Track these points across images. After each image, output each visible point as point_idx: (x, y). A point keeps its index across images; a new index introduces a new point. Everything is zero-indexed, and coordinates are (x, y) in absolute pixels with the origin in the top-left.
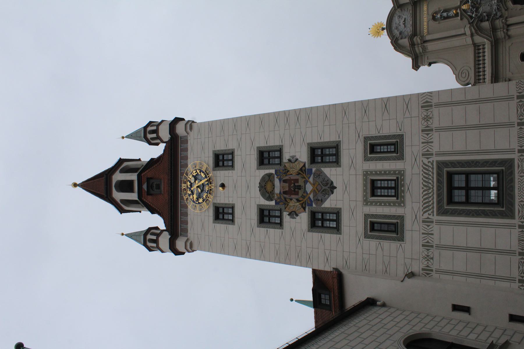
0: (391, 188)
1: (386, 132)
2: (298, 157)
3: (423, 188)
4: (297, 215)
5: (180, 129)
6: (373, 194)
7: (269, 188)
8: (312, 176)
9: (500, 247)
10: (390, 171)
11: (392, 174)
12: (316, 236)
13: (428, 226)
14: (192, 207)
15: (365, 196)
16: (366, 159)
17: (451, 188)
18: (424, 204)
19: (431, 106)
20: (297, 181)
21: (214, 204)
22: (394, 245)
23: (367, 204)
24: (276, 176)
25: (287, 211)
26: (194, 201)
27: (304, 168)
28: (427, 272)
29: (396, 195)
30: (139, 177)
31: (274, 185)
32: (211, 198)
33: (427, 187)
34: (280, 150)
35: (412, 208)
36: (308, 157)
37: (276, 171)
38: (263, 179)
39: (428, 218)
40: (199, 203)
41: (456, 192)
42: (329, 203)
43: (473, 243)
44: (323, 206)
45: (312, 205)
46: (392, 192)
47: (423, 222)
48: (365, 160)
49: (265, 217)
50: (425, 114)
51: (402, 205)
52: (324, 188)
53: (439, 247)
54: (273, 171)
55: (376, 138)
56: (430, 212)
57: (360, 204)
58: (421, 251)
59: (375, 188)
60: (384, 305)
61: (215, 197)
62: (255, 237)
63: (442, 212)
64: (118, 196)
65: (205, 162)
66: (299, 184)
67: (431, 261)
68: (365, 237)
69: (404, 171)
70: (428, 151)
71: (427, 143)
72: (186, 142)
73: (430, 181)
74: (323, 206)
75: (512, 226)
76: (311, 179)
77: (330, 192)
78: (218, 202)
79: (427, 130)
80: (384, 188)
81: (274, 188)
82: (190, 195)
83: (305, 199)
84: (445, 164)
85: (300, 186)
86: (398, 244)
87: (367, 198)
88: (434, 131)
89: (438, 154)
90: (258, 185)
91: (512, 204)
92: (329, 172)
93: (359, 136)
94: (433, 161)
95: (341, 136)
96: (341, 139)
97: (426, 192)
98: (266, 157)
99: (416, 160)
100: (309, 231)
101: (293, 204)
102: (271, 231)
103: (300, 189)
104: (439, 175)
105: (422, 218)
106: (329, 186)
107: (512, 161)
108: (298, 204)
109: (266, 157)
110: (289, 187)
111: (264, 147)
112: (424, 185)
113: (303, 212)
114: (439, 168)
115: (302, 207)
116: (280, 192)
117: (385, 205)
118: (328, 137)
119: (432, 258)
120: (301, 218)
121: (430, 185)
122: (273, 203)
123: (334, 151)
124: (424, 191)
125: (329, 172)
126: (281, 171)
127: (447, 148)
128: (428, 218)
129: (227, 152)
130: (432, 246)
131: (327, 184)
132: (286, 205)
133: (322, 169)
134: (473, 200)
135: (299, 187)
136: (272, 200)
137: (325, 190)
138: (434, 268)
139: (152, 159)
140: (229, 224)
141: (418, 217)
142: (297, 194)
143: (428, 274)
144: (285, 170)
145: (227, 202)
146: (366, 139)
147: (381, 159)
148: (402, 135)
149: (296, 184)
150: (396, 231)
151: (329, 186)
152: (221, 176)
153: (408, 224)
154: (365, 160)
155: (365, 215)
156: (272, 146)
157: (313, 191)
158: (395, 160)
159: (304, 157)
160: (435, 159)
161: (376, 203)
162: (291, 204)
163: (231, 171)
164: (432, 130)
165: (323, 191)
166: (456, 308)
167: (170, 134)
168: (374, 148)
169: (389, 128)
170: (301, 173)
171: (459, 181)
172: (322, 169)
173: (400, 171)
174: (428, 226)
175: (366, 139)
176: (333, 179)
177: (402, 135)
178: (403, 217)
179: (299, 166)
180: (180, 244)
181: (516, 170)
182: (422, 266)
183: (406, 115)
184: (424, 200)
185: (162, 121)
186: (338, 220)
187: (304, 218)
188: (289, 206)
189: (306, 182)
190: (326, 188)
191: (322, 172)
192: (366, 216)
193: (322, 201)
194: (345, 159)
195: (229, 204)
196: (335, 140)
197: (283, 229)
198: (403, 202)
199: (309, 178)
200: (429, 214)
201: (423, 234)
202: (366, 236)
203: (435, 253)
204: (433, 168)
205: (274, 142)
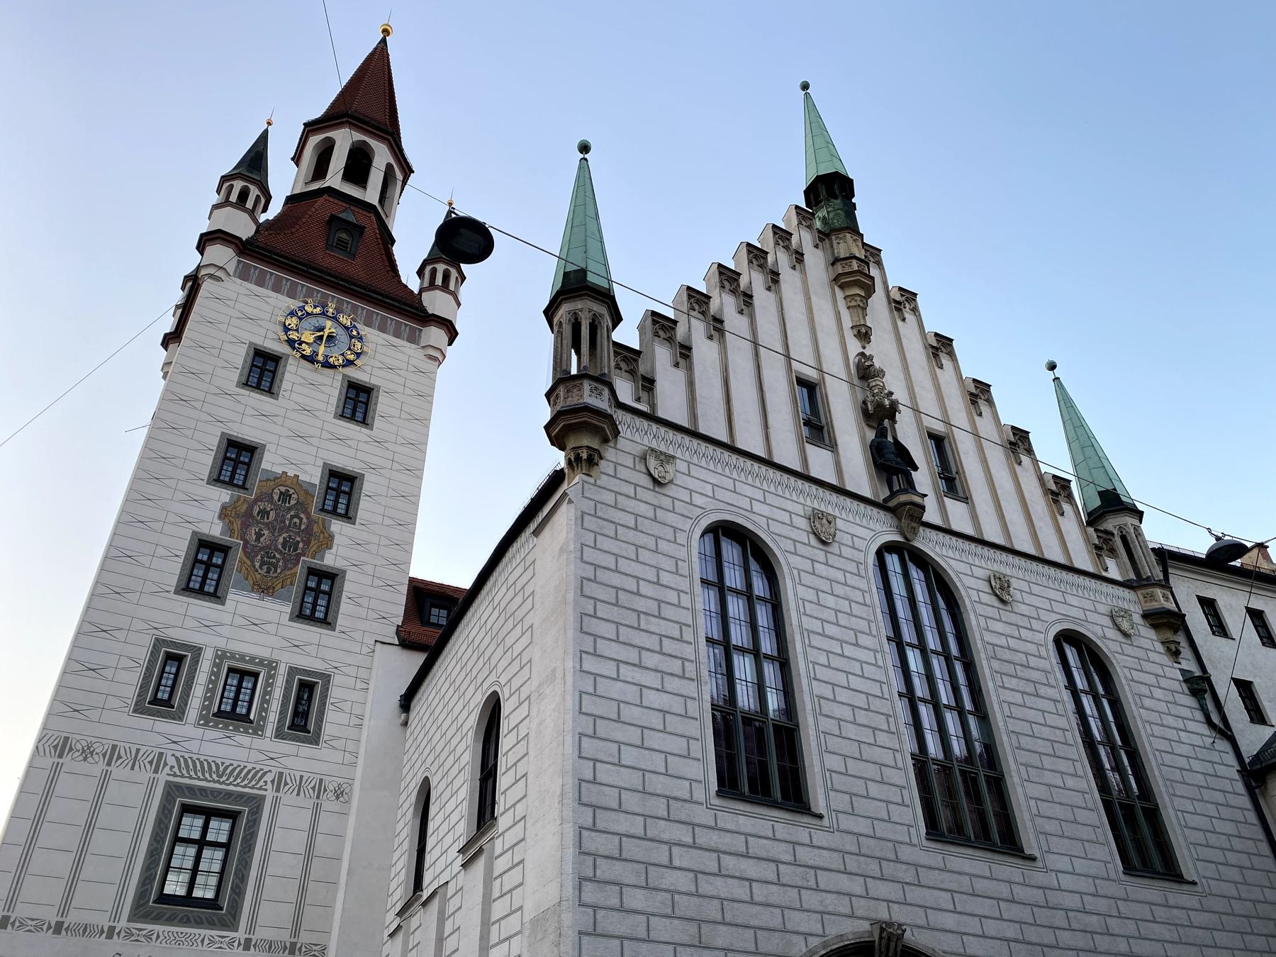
0: (235, 706)
5: (435, 335)
10: (266, 710)
11: (260, 713)
15: (233, 656)
17: (209, 814)
22: (131, 692)
23: (217, 656)
29: (220, 714)
30: (371, 207)
33: (220, 771)
39: (166, 764)
41: (199, 822)
46: (227, 707)
47: (161, 754)
53: (106, 776)
56: (176, 770)
57: (221, 643)
58: (104, 741)
63: (172, 790)
64: (344, 139)
70: (286, 784)
75: (116, 916)
78: (288, 367)
80: (238, 693)
87: (228, 658)
89: (276, 801)
91: (157, 919)
104: (241, 796)
117: (208, 690)
123: (319, 614)
124: (217, 765)
127: (284, 817)
128: (166, 764)
129: (370, 414)
130: (109, 764)
134: (179, 849)
138: (66, 759)
139: (393, 241)
140: (241, 375)
145: (286, 385)
150: (155, 701)
152: (331, 387)
155: (200, 649)
160: (270, 794)
167: (433, 315)
171: (219, 830)
173: (262, 728)
180: (221, 254)
185: (459, 304)
186: (200, 592)
192: (197, 651)
195: (279, 388)
198: (206, 724)
200: (172, 767)
202: (159, 643)
204: (252, 788)
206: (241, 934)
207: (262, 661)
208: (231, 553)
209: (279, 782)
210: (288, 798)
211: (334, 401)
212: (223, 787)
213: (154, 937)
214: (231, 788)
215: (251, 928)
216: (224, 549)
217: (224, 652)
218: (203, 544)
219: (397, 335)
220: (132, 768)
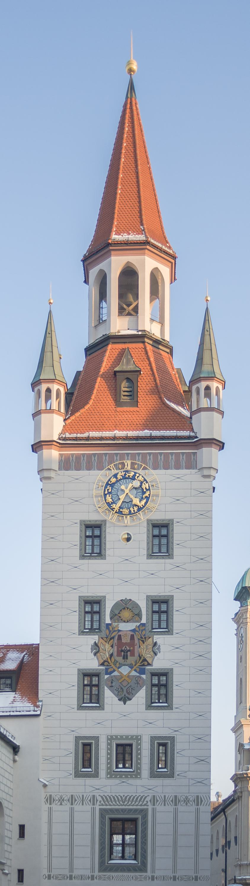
1: (178, 760)
2: (159, 655)
3: (124, 796)
4: (95, 654)
6: (118, 745)
7: (126, 614)
8: (138, 674)
9: (75, 861)
10: (140, 764)
12: (74, 679)
13: (90, 801)
14: (99, 481)
16: (153, 739)
18: (110, 797)
19: (198, 805)
20: (133, 655)
21: (105, 521)
22: (71, 768)
23: (108, 739)
24: (138, 624)
25: (99, 641)
26: (107, 484)
27: (146, 663)
28: (50, 800)
31: (128, 622)
32: (111, 518)
33: (124, 799)
34: (169, 630)
35: (106, 786)
36: (157, 669)
37: (143, 625)
38: (137, 606)
39: (97, 801)
40: (105, 495)
42: (108, 695)
43: (77, 840)
44: (106, 688)
45: (106, 674)
47: (94, 796)
48: (151, 737)
49: (92, 606)
50: (191, 799)
51: (109, 776)
52: (125, 689)
53: (72, 810)
54: (144, 621)
55: (173, 750)
56: (102, 802)
58: (67, 794)
59: (124, 751)
60: (15, 761)
61: (114, 525)
62: (67, 592)
63: (103, 813)
65: (160, 505)
66: (129, 657)
67: (59, 803)
68: (76, 737)
69: (140, 778)
70: (157, 801)
71: (165, 801)
72: (189, 466)
73: (130, 803)
74: (106, 688)
76: (134, 673)
77: (120, 697)
79: (176, 801)
81: (125, 622)
82: (115, 476)
83: (113, 666)
84: (145, 817)
85: (127, 658)
86: (72, 772)
88: (175, 807)
89: (154, 810)
90: (128, 599)
92: (141, 696)
93: (176, 731)
94: (148, 806)
95: (177, 710)
96: (174, 710)
97: (120, 799)
98: (161, 606)
99: (150, 789)
100: (79, 670)
101: (107, 649)
102: (75, 618)
103: (124, 658)
104: (136, 810)
105: (97, 795)
106: (127, 695)
107: (146, 871)
108: (108, 656)
109: (161, 606)
110: (126, 644)
111: (173, 607)
112: (126, 797)
113: (99, 663)
114: (142, 810)
115: (105, 661)
116: (119, 631)
118: (178, 694)
119: (61, 804)
120: (92, 659)
121: (126, 803)
122: (108, 621)
124: (121, 797)
125: (141, 696)
126: (144, 632)
130: (72, 804)
131: (128, 693)
132: (105, 639)
133: (144, 688)
135: (125, 657)
136: (111, 619)
137: (123, 691)
138: (53, 806)
141: (97, 791)
142: (119, 655)
143: (47, 800)
144: (145, 638)
145: (108, 546)
146: (172, 739)
147: (152, 754)
148: (173, 777)
149: (129, 653)
151: (127, 695)
153: (90, 781)
154: (151, 737)
155: (98, 737)
156: (173, 619)
157: (122, 676)
158: (151, 769)
159: (159, 663)
160: (150, 808)
161: (109, 749)
162: (108, 646)
163: (145, 552)
164: (176, 805)
165: (121, 688)
166: (22, 828)
168: (164, 747)
169: (180, 763)
170: (141, 661)
172: (144, 688)
174: (90, 801)
175: (172, 739)
176: (134, 699)
177: (173, 777)
178: (97, 777)
179: (148, 656)
181: (138, 874)
182: (53, 794)
183: (191, 781)
184: (114, 797)
187: (92, 664)
188: (104, 643)
189: (131, 666)
190: (125, 692)
191: (141, 687)
192: (97, 739)
193: (111, 687)
194: (153, 714)
195: (105, 549)
196: (174, 703)
197: (79, 635)
199: (135, 670)
200: (100, 802)
201: (83, 796)
202: (77, 739)
203: (67, 807)
204: (141, 805)
205: (178, 620)
206: (149, 873)
207: (132, 736)
208: (101, 676)
209: (154, 800)
210: (159, 808)
211: (144, 545)
212: (127, 807)
213: (111, 878)
214: (131, 807)
215: (153, 871)
216: (97, 675)
217: (112, 736)
218: (86, 674)
219: (178, 467)
220: (83, 804)
